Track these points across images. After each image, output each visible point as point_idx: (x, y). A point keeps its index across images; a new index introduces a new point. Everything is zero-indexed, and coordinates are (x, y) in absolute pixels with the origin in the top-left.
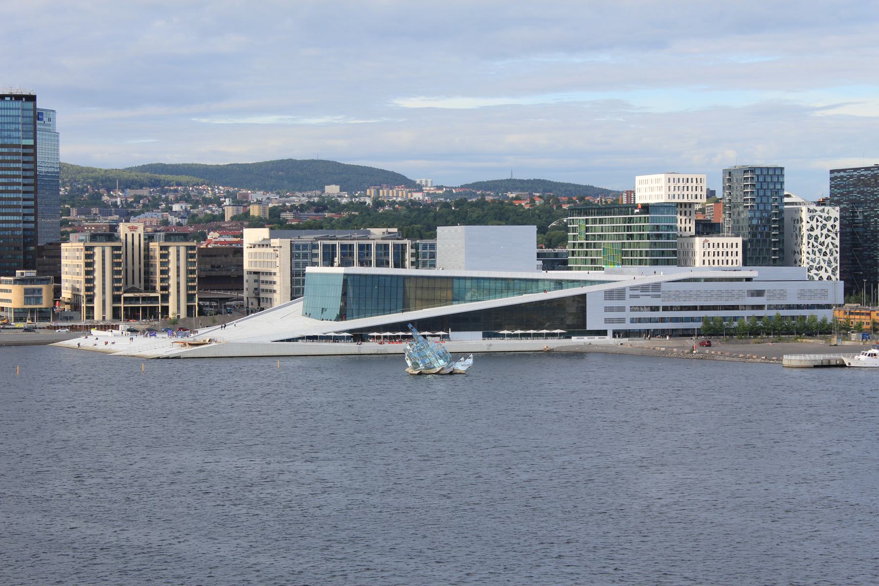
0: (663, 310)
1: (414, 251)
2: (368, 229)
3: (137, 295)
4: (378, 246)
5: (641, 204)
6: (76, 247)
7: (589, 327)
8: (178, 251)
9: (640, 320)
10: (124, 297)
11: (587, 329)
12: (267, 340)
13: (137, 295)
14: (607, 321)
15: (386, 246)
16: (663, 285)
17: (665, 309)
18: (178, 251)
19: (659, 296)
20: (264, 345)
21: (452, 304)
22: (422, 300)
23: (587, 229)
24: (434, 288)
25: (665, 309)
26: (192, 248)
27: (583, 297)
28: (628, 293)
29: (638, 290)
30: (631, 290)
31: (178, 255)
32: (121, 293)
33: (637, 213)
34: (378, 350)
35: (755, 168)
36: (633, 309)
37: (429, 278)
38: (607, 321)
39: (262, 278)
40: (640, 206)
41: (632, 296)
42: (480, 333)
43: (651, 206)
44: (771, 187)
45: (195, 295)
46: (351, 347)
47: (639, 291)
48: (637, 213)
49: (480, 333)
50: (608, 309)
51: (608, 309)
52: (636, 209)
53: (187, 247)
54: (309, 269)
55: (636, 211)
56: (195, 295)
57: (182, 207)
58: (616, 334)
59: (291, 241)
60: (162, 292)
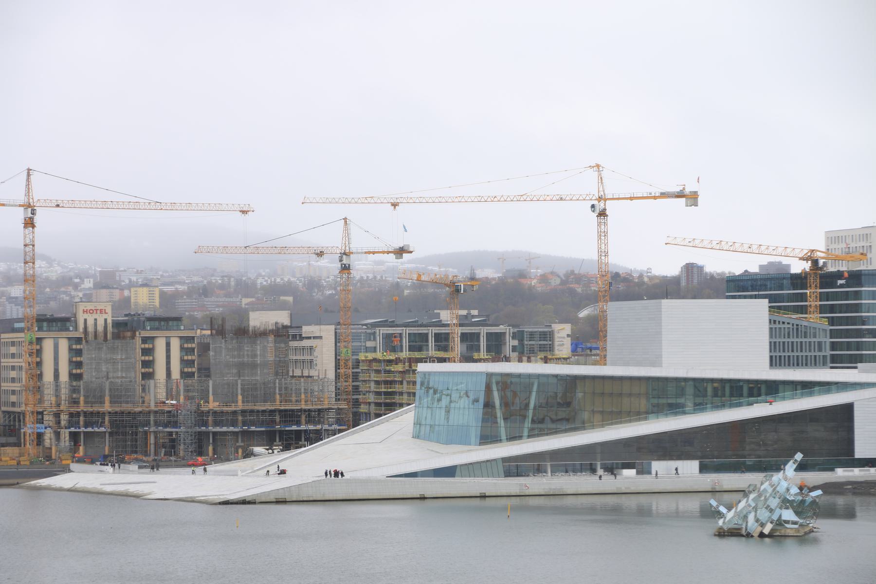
1: (516, 343)
2: (435, 311)
4: (464, 337)
5: (848, 272)
6: (10, 340)
8: (168, 345)
11: (856, 457)
12: (379, 473)
15: (476, 336)
18: (168, 345)
20: (378, 481)
21: (646, 419)
22: (602, 412)
24: (621, 395)
26: (191, 339)
27: (847, 410)
31: (168, 350)
33: (842, 286)
34: (550, 489)
37: (594, 378)
40: (846, 275)
42: (694, 465)
43: (865, 275)
46: (513, 485)
48: (842, 286)
49: (694, 465)
52: (841, 279)
53: (181, 338)
54: (422, 367)
55: (840, 282)
57: (24, 291)
59: (336, 329)
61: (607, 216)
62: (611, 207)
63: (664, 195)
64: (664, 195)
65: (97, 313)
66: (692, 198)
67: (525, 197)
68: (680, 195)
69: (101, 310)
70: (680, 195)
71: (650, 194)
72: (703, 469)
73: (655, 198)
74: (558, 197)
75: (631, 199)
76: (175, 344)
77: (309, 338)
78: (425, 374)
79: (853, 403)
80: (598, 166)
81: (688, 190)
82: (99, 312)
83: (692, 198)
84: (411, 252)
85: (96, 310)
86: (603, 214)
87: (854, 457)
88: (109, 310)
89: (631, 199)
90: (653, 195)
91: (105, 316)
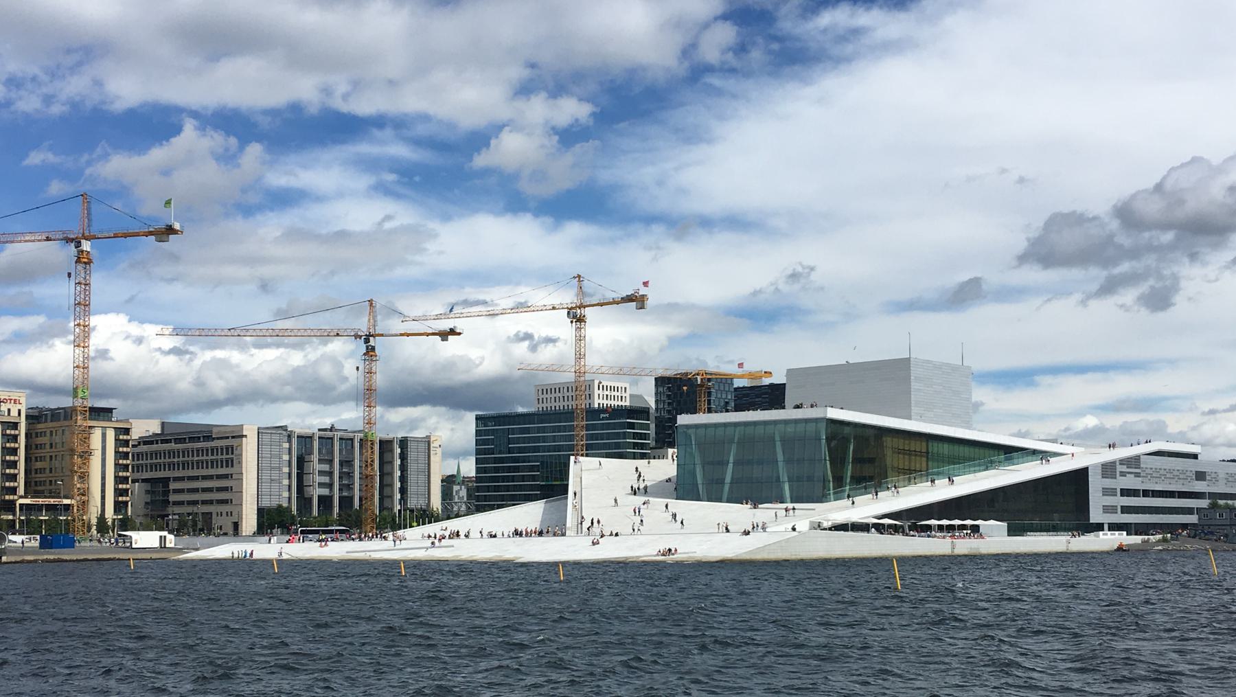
0: (1143, 496)
3: (41, 501)
7: (1095, 516)
8: (104, 436)
9: (1126, 510)
10: (20, 504)
11: (1091, 522)
13: (41, 501)
14: (1108, 509)
16: (1141, 456)
17: (1146, 493)
18: (104, 436)
19: (1137, 475)
23: (510, 441)
25: (1146, 493)
28: (1120, 468)
29: (1124, 464)
30: (1120, 464)
32: (16, 497)
36: (1126, 493)
38: (1108, 509)
39: (173, 486)
41: (1123, 474)
44: (724, 396)
45: (126, 503)
47: (1125, 466)
50: (1108, 492)
51: (1108, 492)
56: (126, 503)
58: (1114, 527)
60: (78, 498)
61: (585, 322)
62: (588, 312)
65: (10, 403)
69: (15, 400)
72: (1013, 531)
76: (111, 435)
77: (228, 438)
78: (688, 427)
79: (1087, 468)
82: (12, 401)
85: (11, 400)
87: (1089, 521)
88: (23, 400)
91: (19, 407)
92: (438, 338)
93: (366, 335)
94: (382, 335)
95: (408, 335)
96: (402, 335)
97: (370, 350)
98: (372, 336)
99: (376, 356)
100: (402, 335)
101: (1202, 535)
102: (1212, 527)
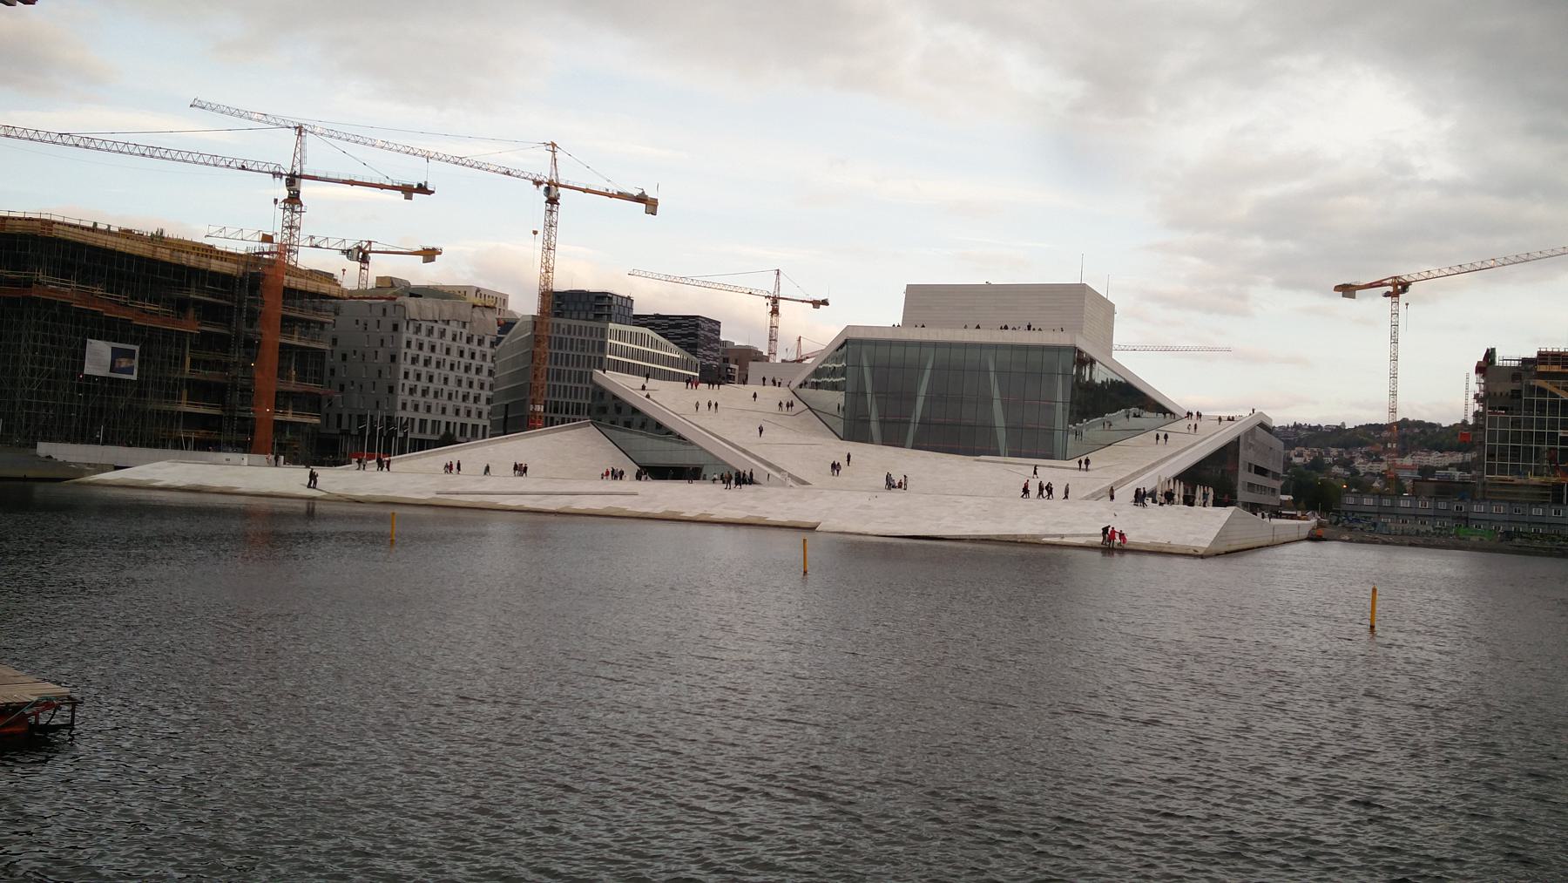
35: (613, 295)
61: (558, 204)
63: (621, 196)
64: (621, 196)
66: (651, 206)
67: (464, 161)
68: (641, 199)
70: (641, 199)
71: (607, 190)
73: (611, 196)
74: (503, 170)
75: (586, 191)
80: (554, 145)
81: (650, 194)
83: (651, 206)
84: (433, 192)
86: (553, 201)
89: (586, 191)
90: (610, 192)
92: (399, 195)
93: (290, 175)
94: (314, 178)
95: (352, 183)
96: (345, 182)
97: (294, 200)
98: (297, 177)
99: (301, 205)
100: (345, 182)
101: (1346, 522)
102: (1356, 514)
